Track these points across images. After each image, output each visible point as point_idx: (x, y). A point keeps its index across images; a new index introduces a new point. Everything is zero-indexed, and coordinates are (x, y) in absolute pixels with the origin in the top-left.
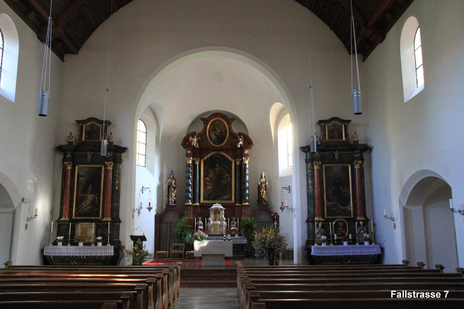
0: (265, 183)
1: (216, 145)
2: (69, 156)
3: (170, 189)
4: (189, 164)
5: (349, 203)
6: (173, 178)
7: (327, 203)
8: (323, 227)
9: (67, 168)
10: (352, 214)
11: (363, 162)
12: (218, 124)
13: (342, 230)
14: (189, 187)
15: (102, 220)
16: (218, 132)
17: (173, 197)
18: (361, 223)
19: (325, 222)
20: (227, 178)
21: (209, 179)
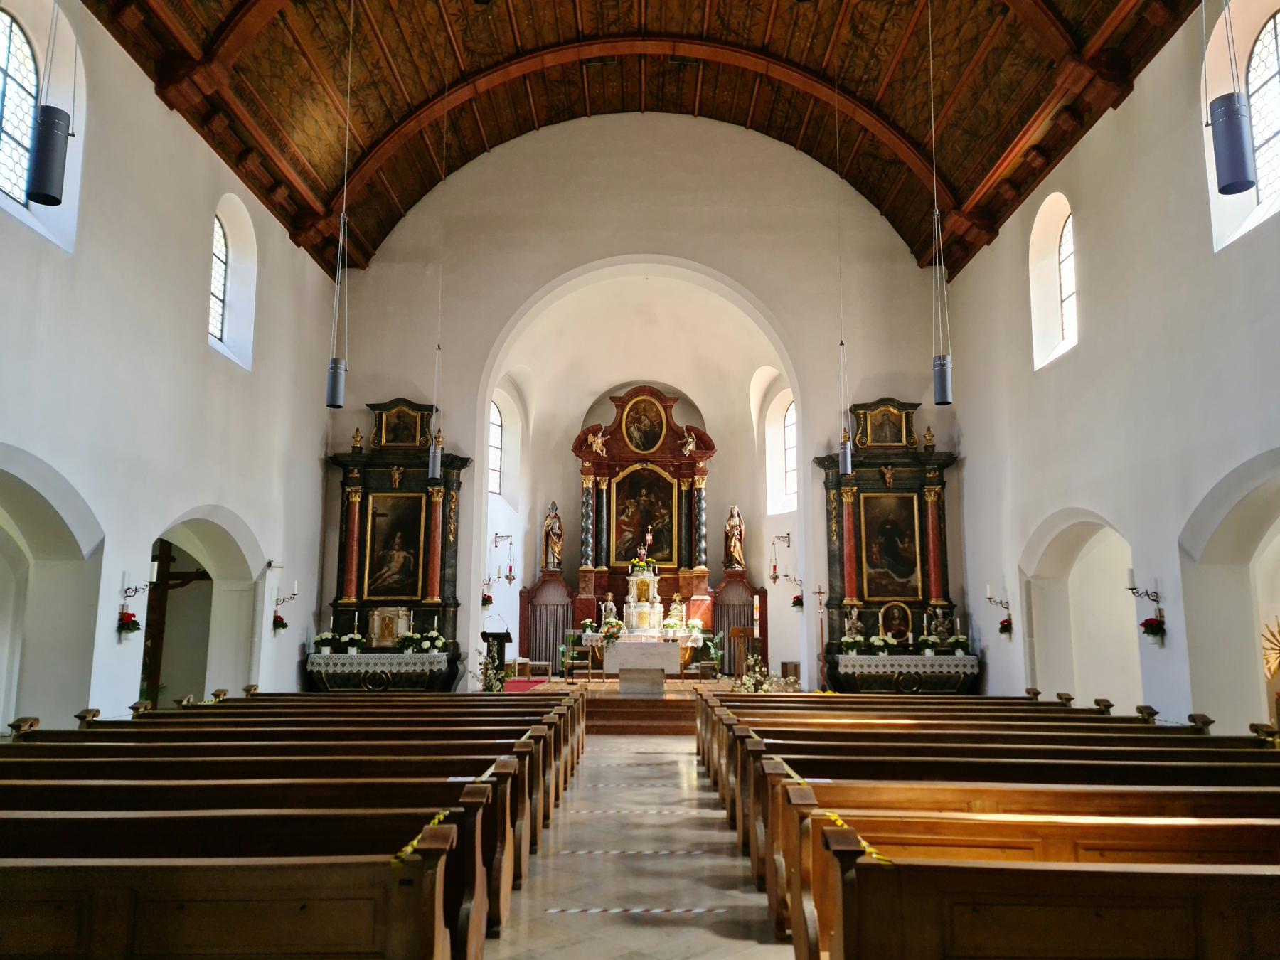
0: (740, 526)
1: (643, 450)
2: (356, 474)
3: (550, 538)
4: (587, 489)
5: (913, 571)
6: (556, 516)
7: (867, 571)
8: (860, 617)
9: (351, 500)
10: (920, 593)
11: (943, 488)
12: (644, 409)
13: (900, 625)
14: (587, 534)
15: (423, 602)
16: (644, 425)
17: (556, 554)
18: (937, 610)
19: (864, 608)
20: (663, 516)
21: (626, 519)
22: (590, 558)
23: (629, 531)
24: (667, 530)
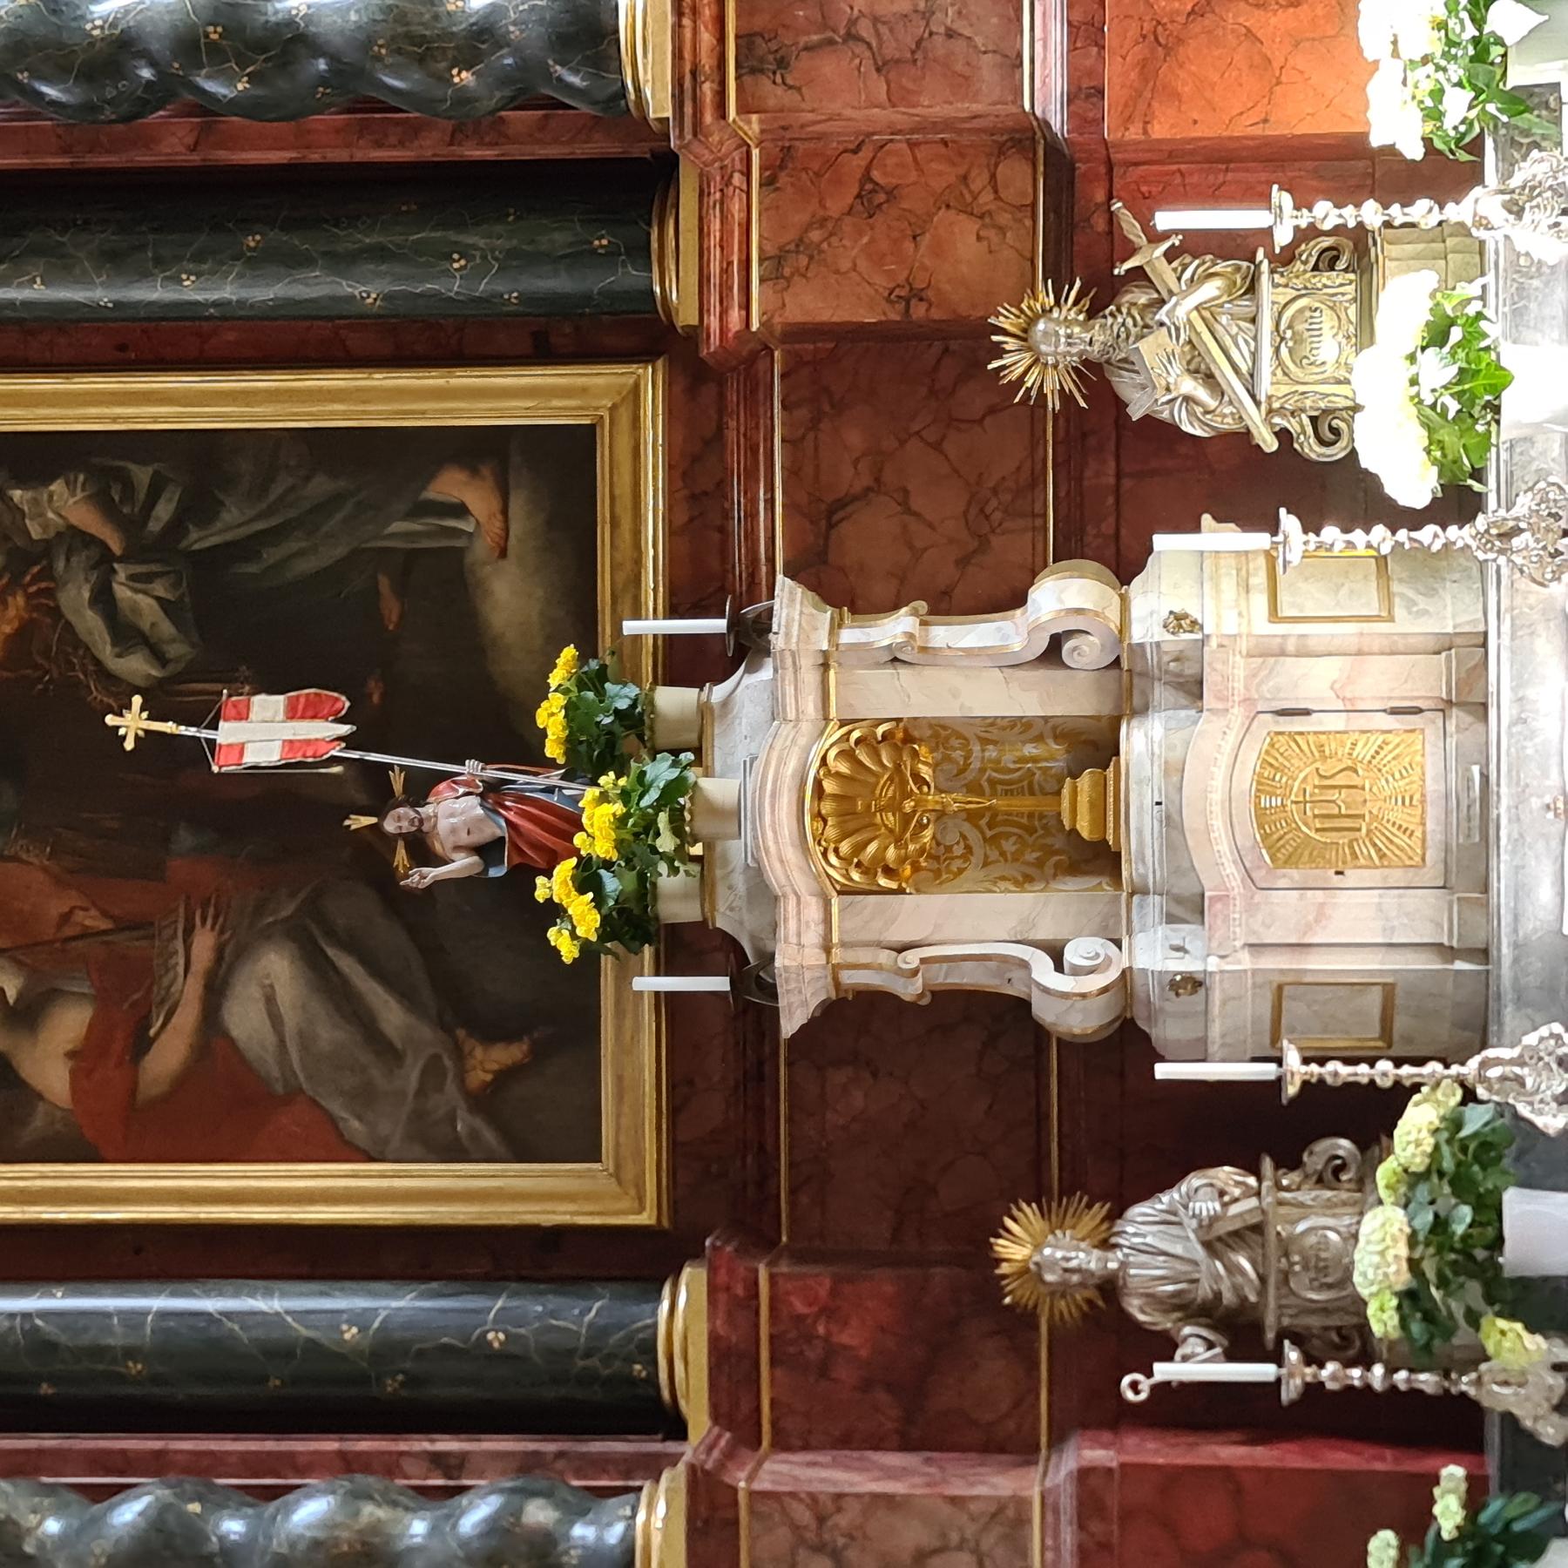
22: (539, 1513)
23: (216, 990)
24: (197, 508)
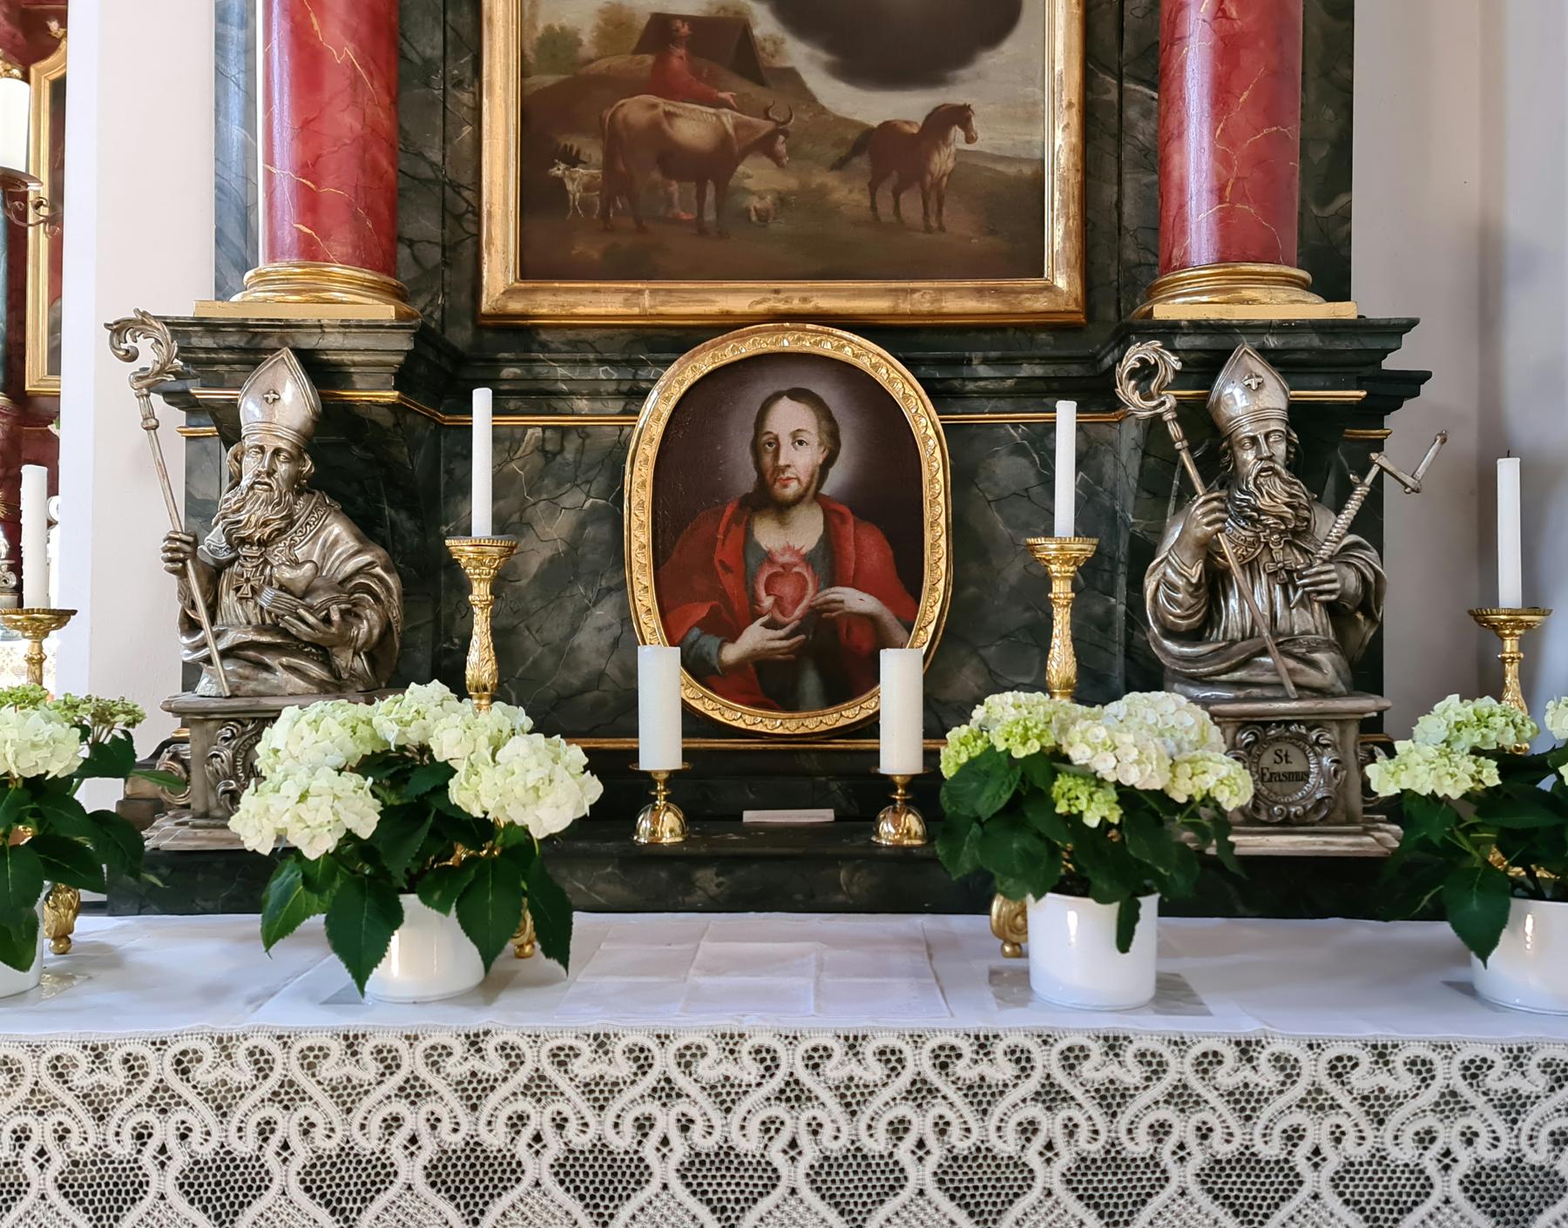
10: (1058, 234)
